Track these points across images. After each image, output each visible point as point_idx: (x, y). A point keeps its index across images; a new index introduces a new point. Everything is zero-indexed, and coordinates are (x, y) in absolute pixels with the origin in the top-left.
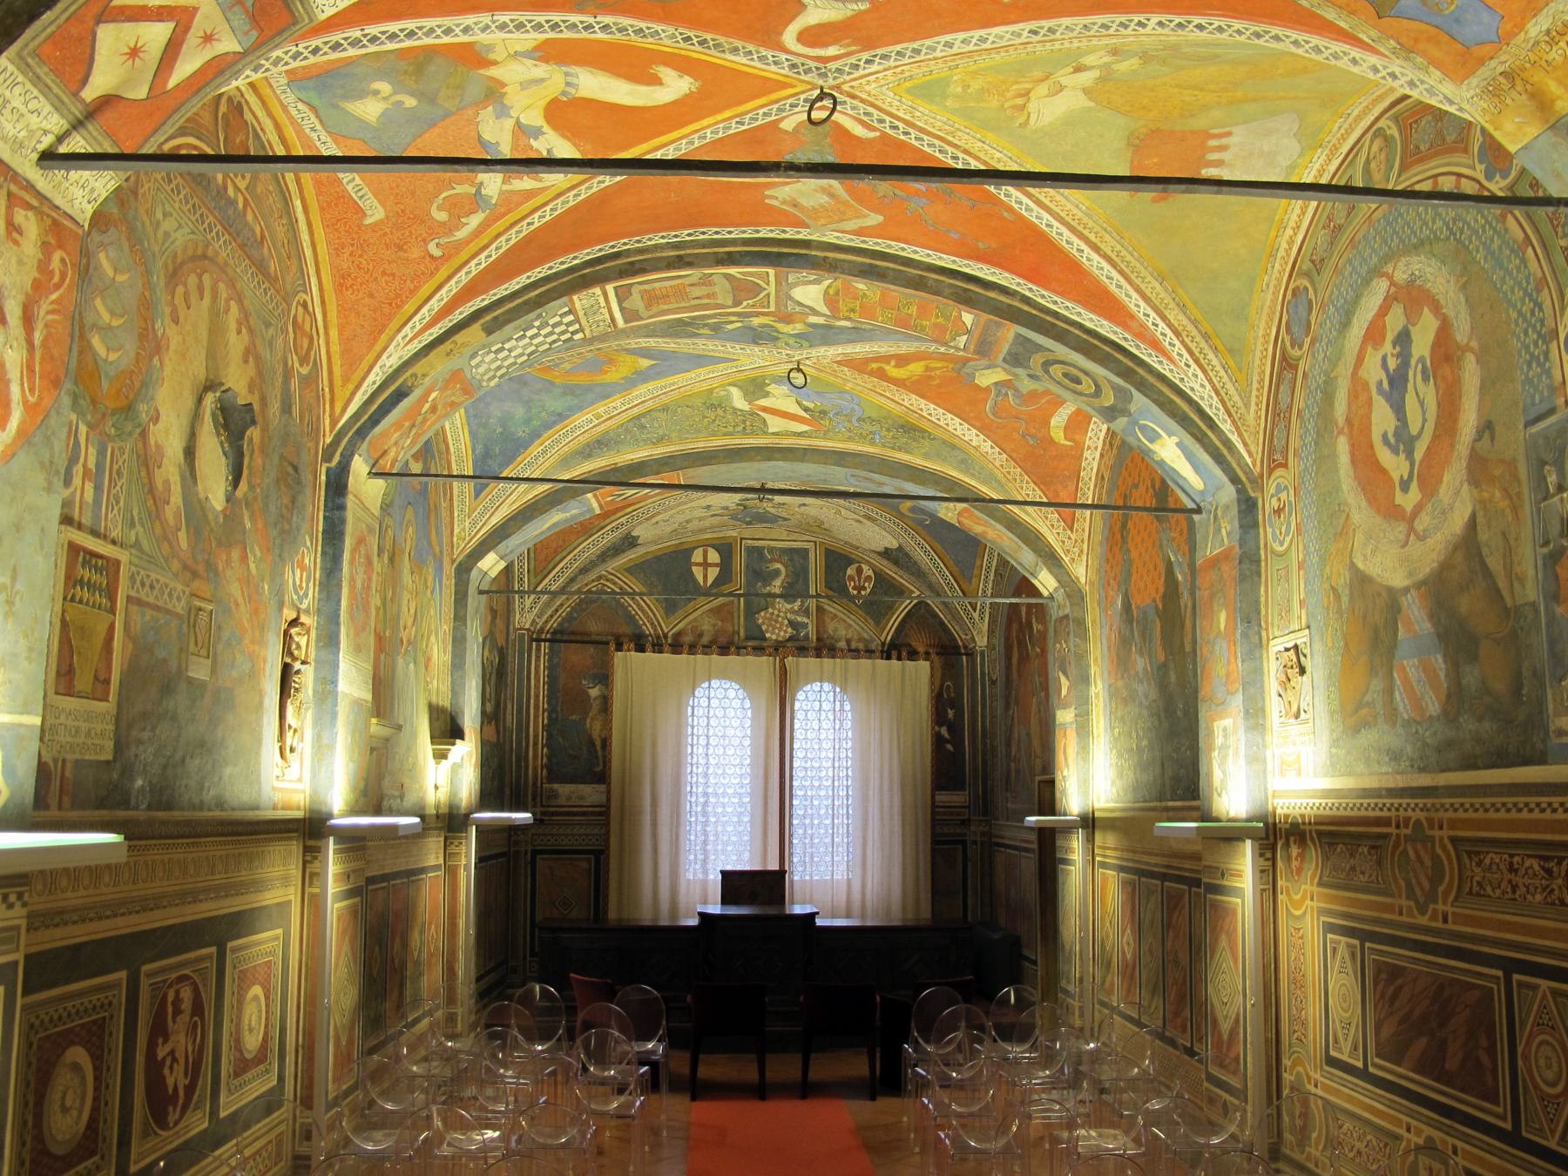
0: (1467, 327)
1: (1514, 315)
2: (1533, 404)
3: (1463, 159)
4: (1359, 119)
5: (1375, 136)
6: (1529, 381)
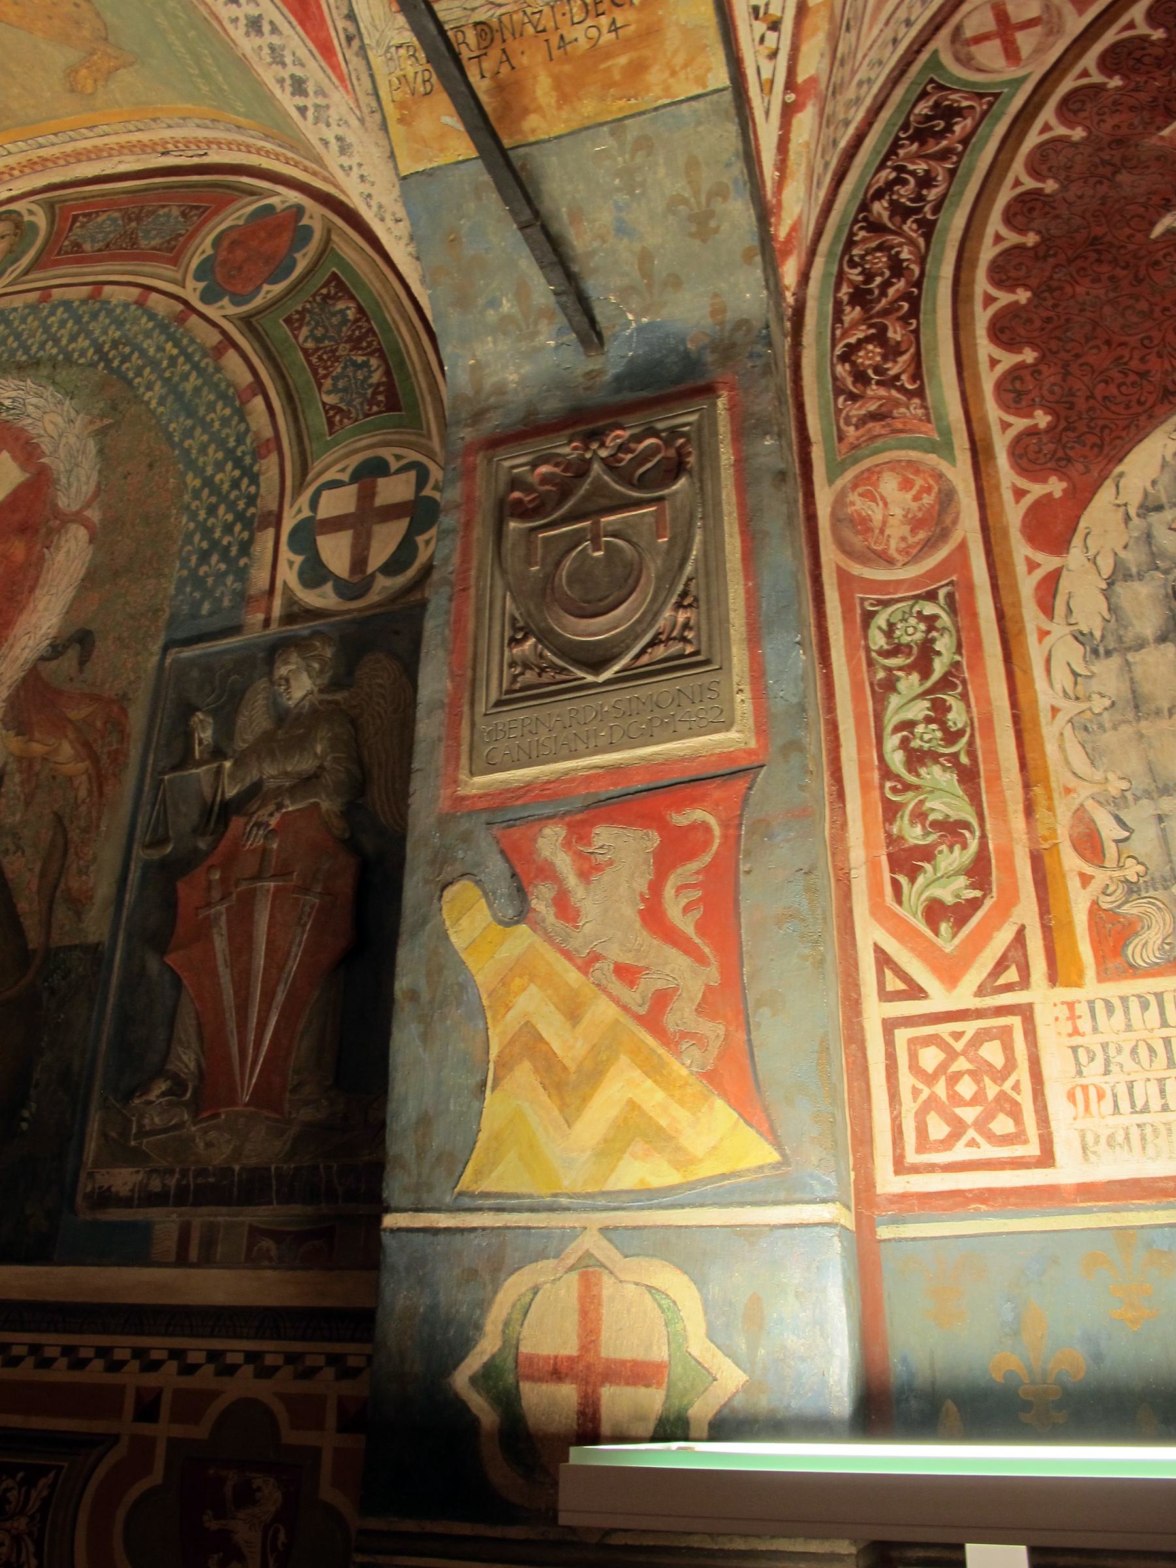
0: (88, 489)
1: (197, 483)
2: (194, 616)
3: (168, 271)
6: (198, 582)
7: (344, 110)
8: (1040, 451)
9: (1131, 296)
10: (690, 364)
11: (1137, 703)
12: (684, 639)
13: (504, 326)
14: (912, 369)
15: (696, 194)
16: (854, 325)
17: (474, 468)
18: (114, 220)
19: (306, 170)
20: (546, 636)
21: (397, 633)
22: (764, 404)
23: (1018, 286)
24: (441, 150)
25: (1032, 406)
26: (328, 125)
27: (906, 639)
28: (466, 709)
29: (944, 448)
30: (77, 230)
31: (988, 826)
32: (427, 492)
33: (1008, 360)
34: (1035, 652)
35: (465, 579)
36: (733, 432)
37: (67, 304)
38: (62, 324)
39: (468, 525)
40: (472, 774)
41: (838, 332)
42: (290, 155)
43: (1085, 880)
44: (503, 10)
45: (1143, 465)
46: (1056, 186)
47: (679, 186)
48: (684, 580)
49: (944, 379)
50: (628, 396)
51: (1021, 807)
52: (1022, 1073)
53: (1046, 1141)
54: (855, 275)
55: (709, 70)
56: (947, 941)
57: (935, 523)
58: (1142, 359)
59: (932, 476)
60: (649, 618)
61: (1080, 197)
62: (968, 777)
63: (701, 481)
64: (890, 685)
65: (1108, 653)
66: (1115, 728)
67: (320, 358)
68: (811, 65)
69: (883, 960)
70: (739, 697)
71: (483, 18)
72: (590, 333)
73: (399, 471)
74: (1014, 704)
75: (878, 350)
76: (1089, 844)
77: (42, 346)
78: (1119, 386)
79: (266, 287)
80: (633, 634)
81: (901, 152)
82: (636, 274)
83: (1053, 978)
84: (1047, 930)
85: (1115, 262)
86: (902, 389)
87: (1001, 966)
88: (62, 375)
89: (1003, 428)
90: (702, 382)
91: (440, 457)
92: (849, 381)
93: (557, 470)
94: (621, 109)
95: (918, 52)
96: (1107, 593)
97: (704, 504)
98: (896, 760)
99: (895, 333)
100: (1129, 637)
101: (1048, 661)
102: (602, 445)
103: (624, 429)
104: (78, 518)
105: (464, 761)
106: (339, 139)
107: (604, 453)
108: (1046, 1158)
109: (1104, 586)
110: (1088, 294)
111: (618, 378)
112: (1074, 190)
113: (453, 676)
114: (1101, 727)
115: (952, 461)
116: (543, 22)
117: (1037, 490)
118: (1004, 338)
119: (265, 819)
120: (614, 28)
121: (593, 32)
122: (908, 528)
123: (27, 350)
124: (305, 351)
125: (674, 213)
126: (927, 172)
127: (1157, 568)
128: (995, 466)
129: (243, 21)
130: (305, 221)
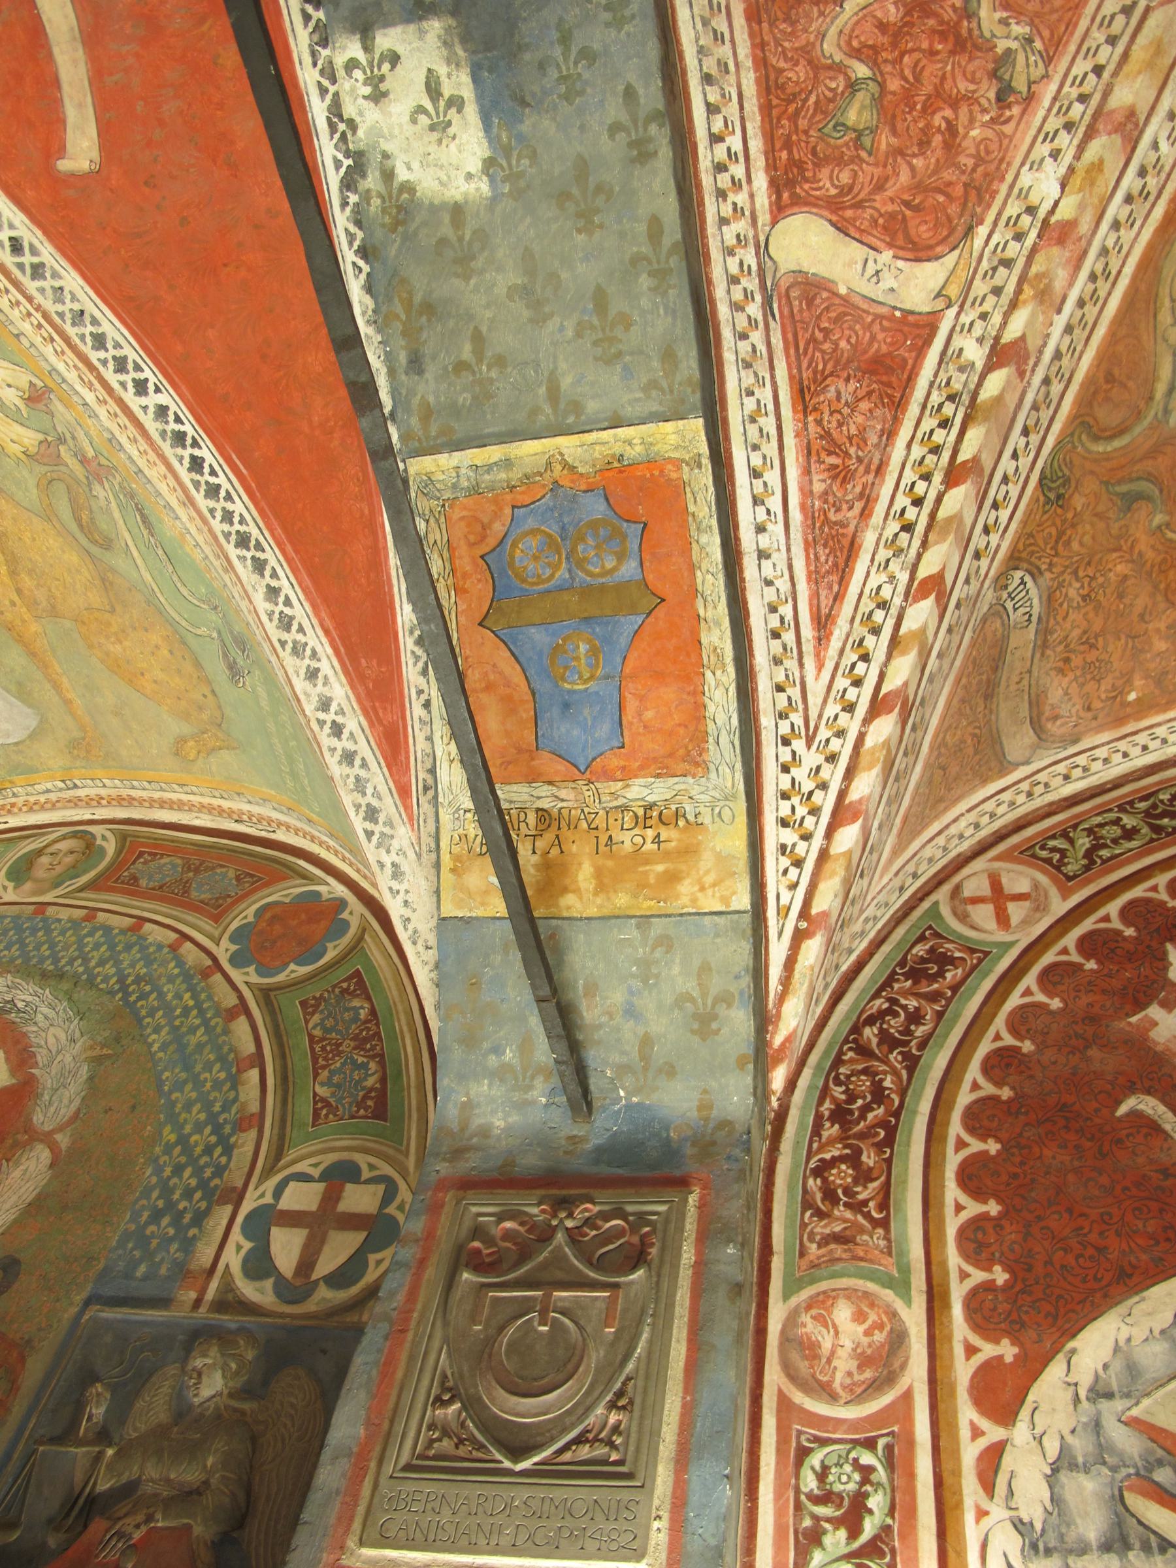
0: (66, 1112)
1: (173, 1138)
2: (128, 1275)
3: (207, 925)
4: (76, 803)
5: (75, 835)
6: (143, 1241)
7: (405, 843)
8: (994, 1309)
10: (671, 1152)
12: (611, 1444)
13: (501, 1074)
14: (880, 1197)
15: (704, 995)
16: (831, 1142)
17: (442, 1206)
18: (174, 866)
19: (358, 871)
20: (473, 1405)
21: (324, 1352)
22: (733, 1210)
23: (989, 1136)
24: (483, 904)
26: (388, 852)
27: (838, 1487)
28: (373, 1465)
29: (902, 1286)
30: (139, 865)
32: (391, 1210)
33: (973, 1208)
34: (972, 1533)
35: (407, 1320)
36: (698, 1232)
37: (107, 929)
38: (97, 946)
39: (422, 1262)
40: (361, 1543)
41: (815, 1145)
42: (347, 855)
44: (564, 804)
45: (1095, 1345)
46: (1033, 1048)
47: (690, 986)
48: (622, 1378)
49: (909, 1213)
50: (605, 1170)
54: (838, 1092)
55: (734, 893)
57: (882, 1363)
58: (1101, 1233)
59: (886, 1313)
60: (580, 1411)
61: (1054, 1063)
63: (659, 1275)
64: (814, 1537)
67: (323, 1048)
68: (826, 900)
70: (656, 1524)
71: (546, 806)
72: (579, 1088)
73: (368, 1181)
75: (850, 1171)
77: (71, 962)
78: (1077, 1257)
79: (292, 966)
80: (560, 1426)
81: (896, 986)
82: (635, 1055)
86: (867, 1216)
88: (80, 995)
89: (963, 1278)
90: (677, 1173)
91: (413, 1178)
92: (819, 1196)
93: (522, 1229)
94: (650, 908)
95: (921, 900)
96: (1052, 1479)
97: (657, 1301)
99: (869, 1158)
100: (1071, 1537)
101: (984, 1546)
102: (570, 1215)
103: (594, 1203)
104: (47, 1138)
105: (357, 1525)
106: (394, 865)
107: (570, 1224)
109: (1049, 1472)
110: (1054, 1157)
111: (599, 1150)
112: (1049, 1055)
113: (368, 1423)
115: (908, 1302)
116: (597, 821)
117: (989, 1350)
119: (130, 1529)
120: (657, 839)
121: (638, 840)
122: (856, 1363)
123: (56, 961)
124: (311, 1038)
125: (680, 1008)
126: (917, 1009)
127: (1104, 1463)
128: (950, 1316)
129: (339, 752)
130: (345, 915)
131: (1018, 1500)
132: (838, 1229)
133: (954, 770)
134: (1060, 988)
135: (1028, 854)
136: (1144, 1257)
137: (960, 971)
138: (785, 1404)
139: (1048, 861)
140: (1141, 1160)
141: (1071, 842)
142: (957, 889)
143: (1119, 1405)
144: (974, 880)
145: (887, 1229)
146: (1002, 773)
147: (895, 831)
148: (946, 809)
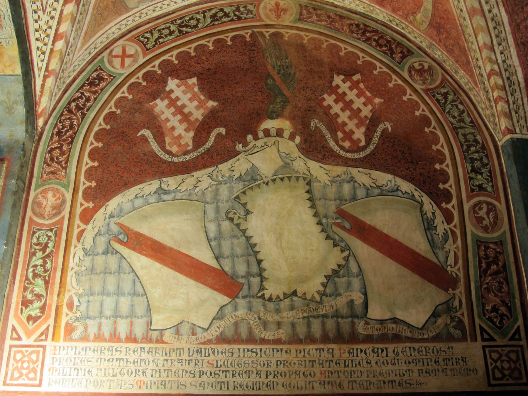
9: (126, 153)
11: (92, 270)
15: (9, 101)
16: (55, 142)
23: (100, 141)
25: (92, 180)
27: (42, 241)
29: (67, 187)
31: (48, 297)
33: (91, 164)
34: (72, 251)
43: (67, 315)
45: (113, 204)
51: (57, 293)
52: (40, 363)
53: (41, 381)
54: (60, 125)
55: (16, 69)
56: (31, 326)
57: (58, 209)
61: (124, 118)
62: (47, 283)
64: (34, 254)
65: (89, 255)
66: (85, 276)
68: (54, 65)
69: (14, 329)
74: (63, 265)
76: (70, 306)
81: (84, 88)
83: (53, 339)
84: (55, 327)
85: (125, 141)
86: (61, 166)
87: (41, 334)
89: (84, 184)
92: (49, 159)
95: (99, 55)
96: (94, 238)
98: (30, 275)
99: (65, 148)
108: (40, 385)
114: (82, 275)
115: (68, 192)
117: (86, 205)
118: (92, 157)
122: (51, 209)
126: (89, 97)
127: (108, 234)
131: (85, 243)
132: (53, 170)
133: (106, 13)
134: (133, 91)
135: (137, 39)
136: (132, 179)
137: (105, 83)
138: (31, 220)
139: (142, 42)
140: (140, 150)
141: (152, 34)
142: (112, 51)
143: (115, 219)
144: (117, 50)
145: (66, 170)
146: (127, 12)
147: (82, 38)
148: (104, 27)
